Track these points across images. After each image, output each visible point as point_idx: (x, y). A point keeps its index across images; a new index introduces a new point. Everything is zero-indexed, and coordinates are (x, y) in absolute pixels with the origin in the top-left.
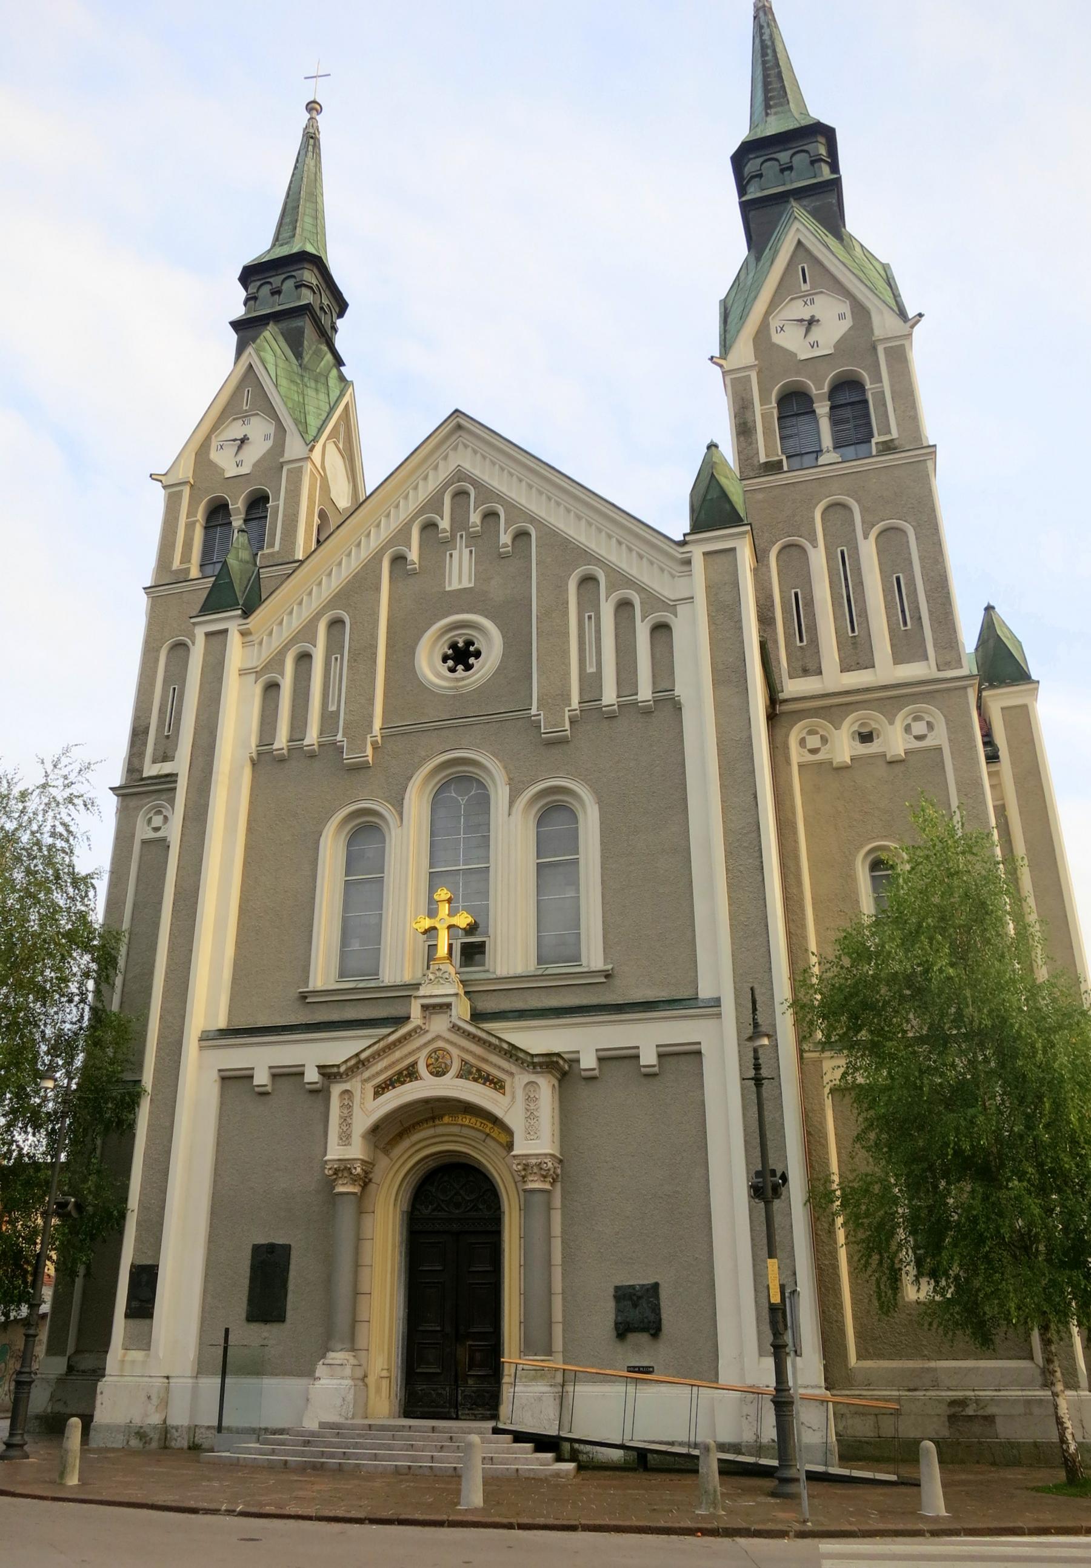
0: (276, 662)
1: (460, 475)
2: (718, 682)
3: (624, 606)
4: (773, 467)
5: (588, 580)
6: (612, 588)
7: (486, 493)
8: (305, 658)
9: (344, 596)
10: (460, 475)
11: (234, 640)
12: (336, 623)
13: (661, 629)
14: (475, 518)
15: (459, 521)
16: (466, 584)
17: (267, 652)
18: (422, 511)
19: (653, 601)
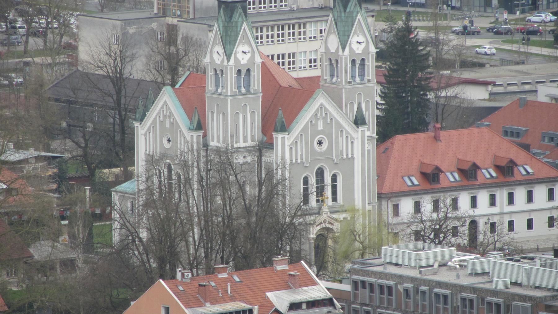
0: (292, 144)
1: (322, 104)
2: (362, 156)
3: (347, 137)
4: (350, 82)
5: (342, 131)
6: (346, 134)
7: (326, 109)
8: (296, 142)
9: (302, 130)
10: (322, 104)
11: (286, 138)
12: (301, 135)
13: (352, 142)
14: (324, 115)
15: (321, 115)
16: (322, 129)
17: (291, 142)
18: (315, 112)
19: (352, 138)
